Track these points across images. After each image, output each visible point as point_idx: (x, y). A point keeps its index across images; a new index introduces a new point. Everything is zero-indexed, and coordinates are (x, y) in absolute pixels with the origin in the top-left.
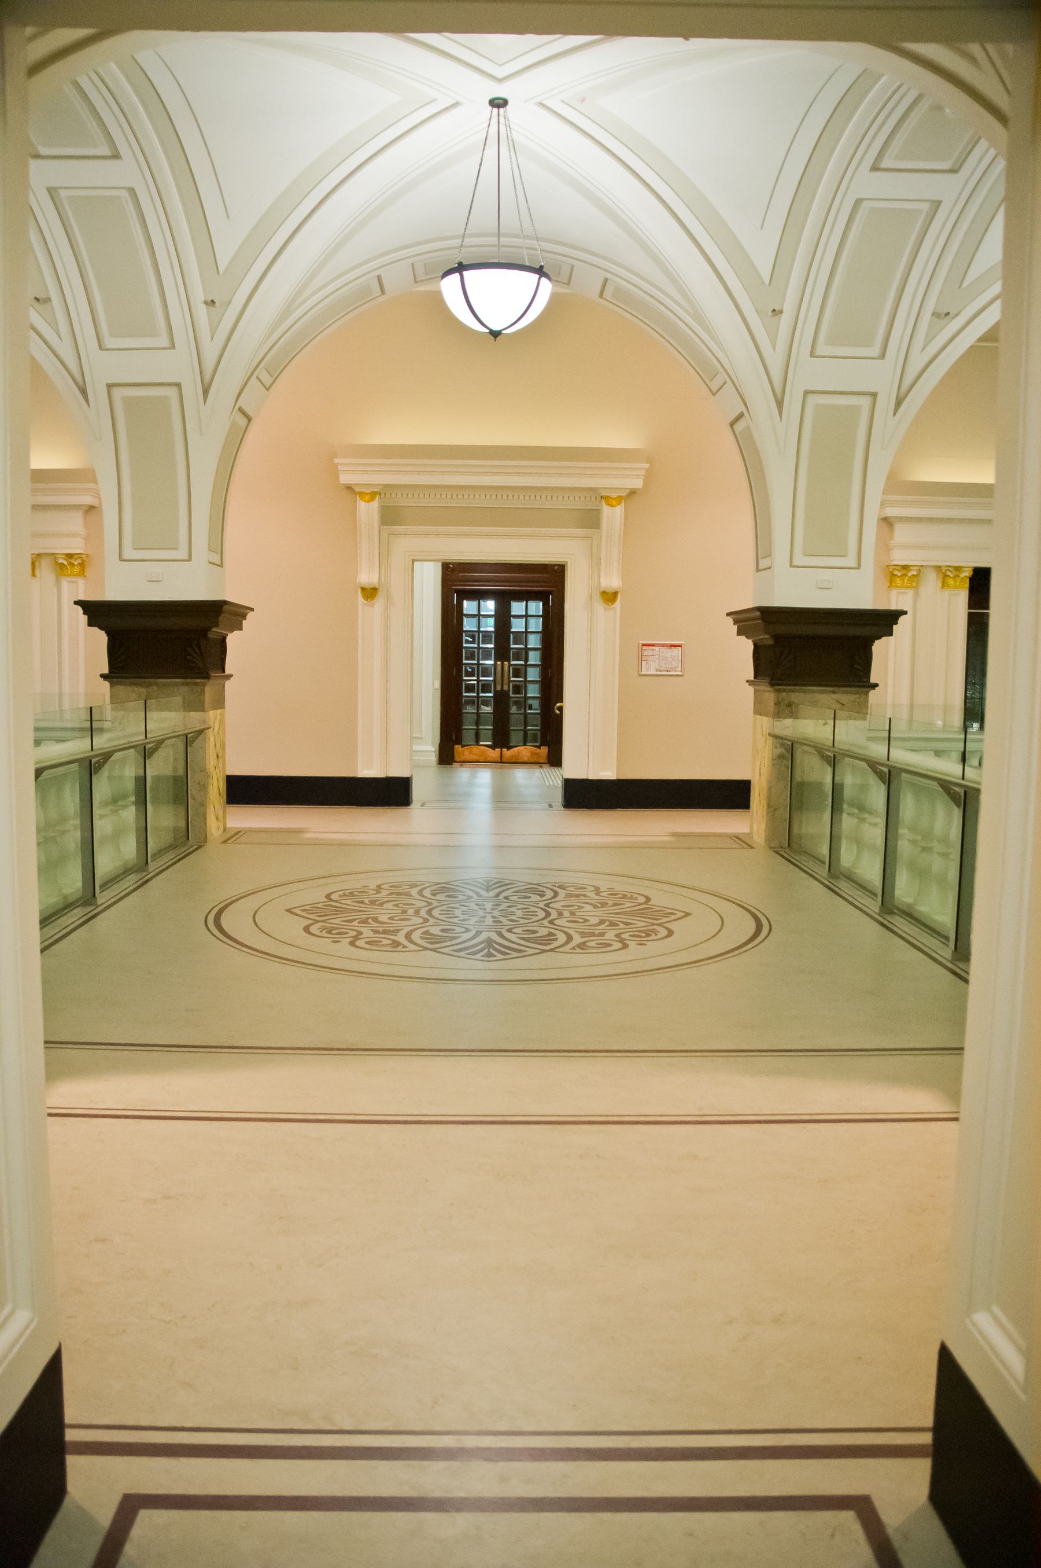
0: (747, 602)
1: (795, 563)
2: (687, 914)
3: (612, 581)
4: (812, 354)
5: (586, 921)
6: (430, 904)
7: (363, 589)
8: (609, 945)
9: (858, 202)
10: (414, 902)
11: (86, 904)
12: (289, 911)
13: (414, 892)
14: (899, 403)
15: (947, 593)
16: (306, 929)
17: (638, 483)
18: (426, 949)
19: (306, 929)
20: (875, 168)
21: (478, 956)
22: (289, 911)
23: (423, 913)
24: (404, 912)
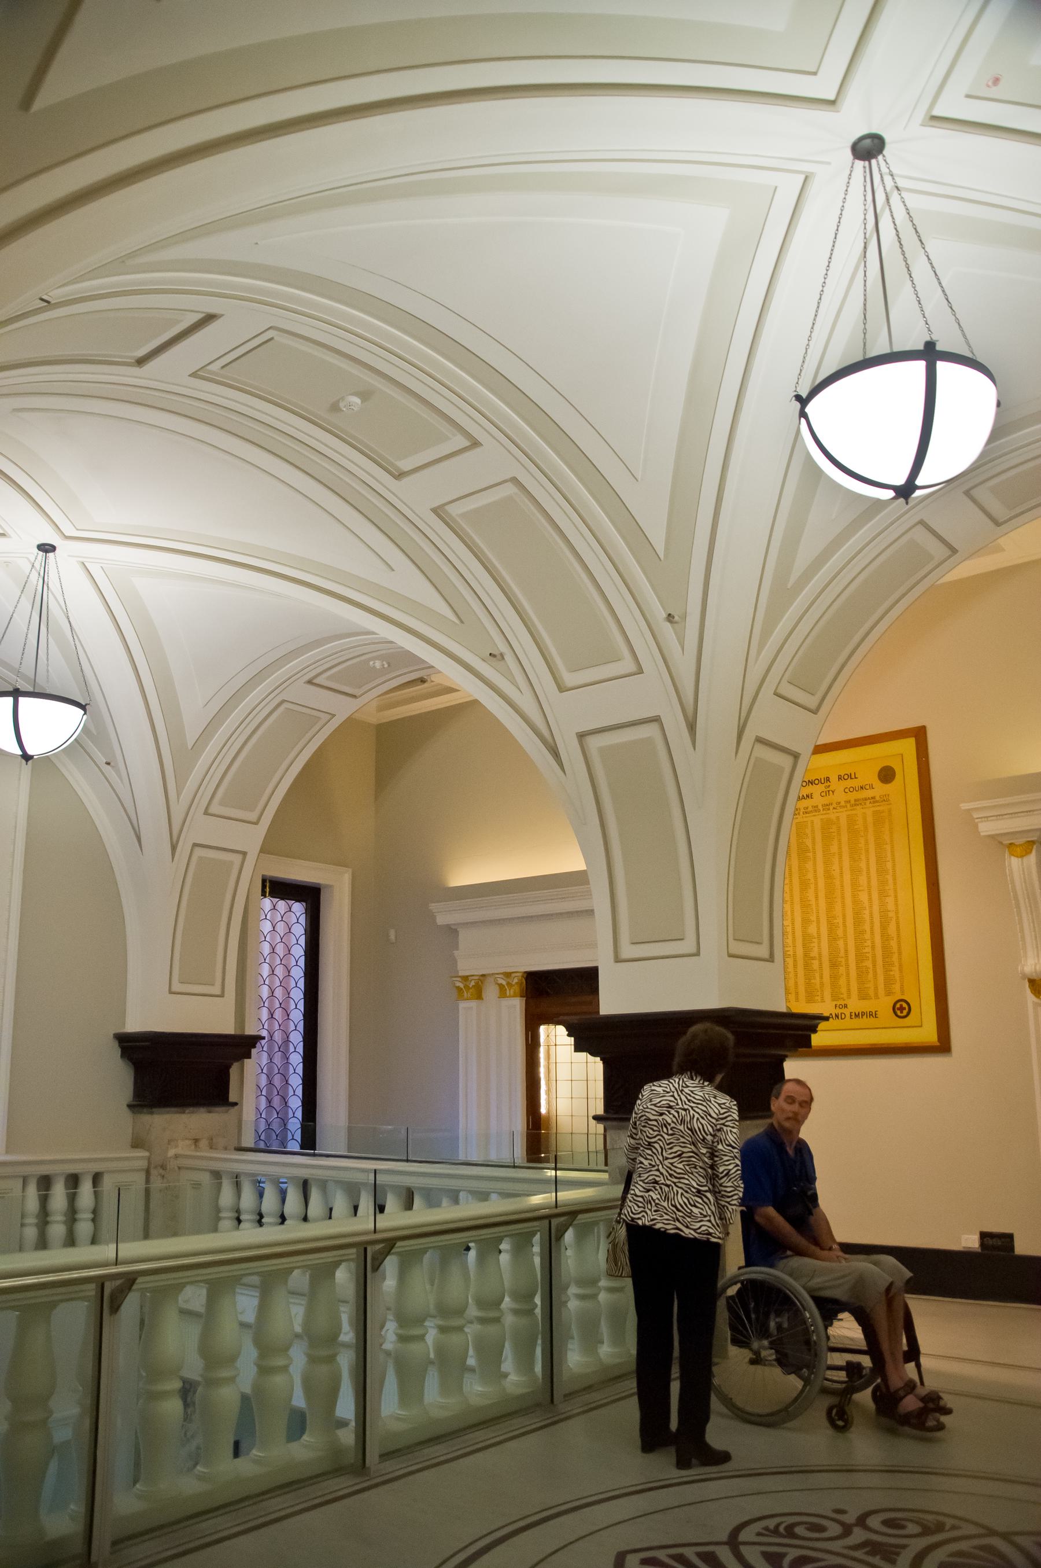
7: (1032, 982)
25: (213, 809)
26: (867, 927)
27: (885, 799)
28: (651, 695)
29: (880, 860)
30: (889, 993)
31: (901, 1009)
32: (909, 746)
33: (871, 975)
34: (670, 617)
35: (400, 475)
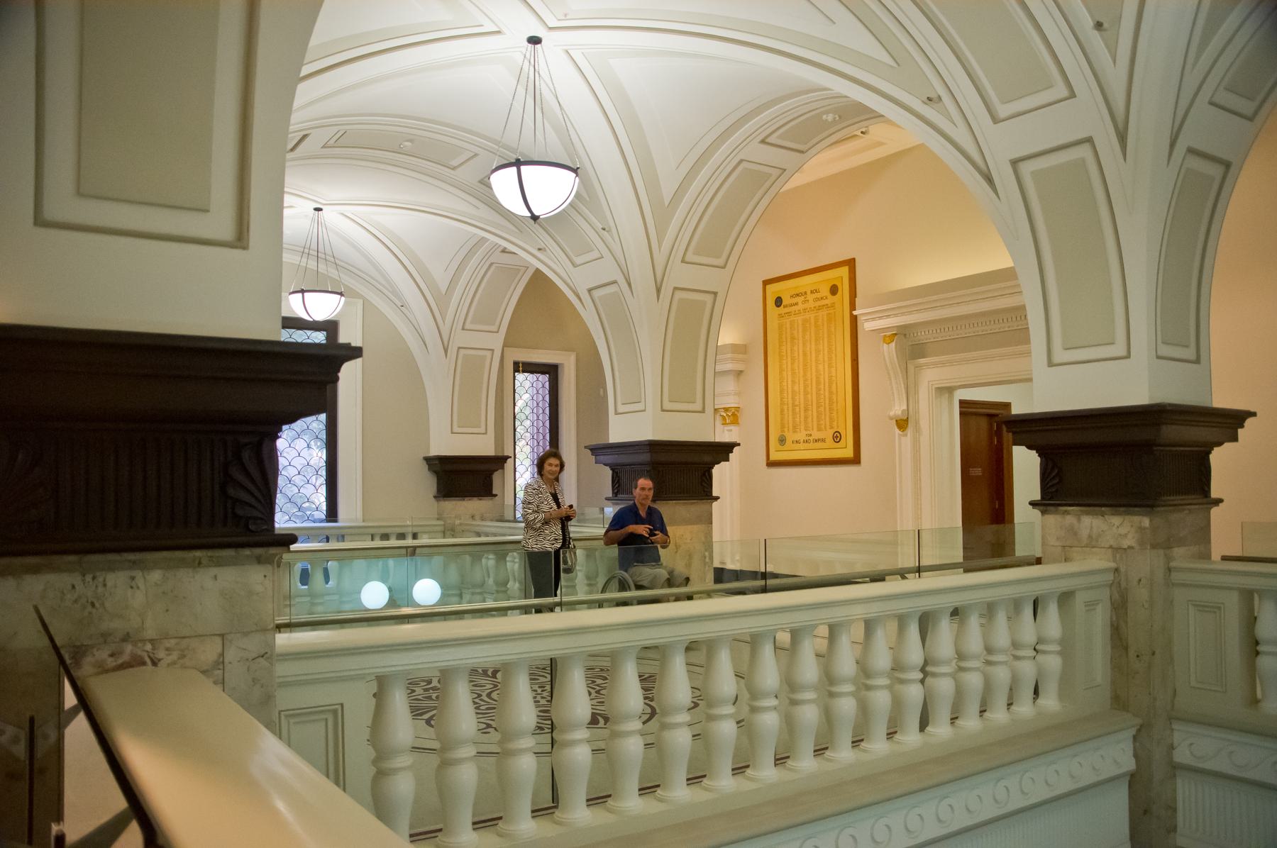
25: (467, 326)
27: (833, 305)
29: (829, 342)
30: (832, 428)
31: (837, 437)
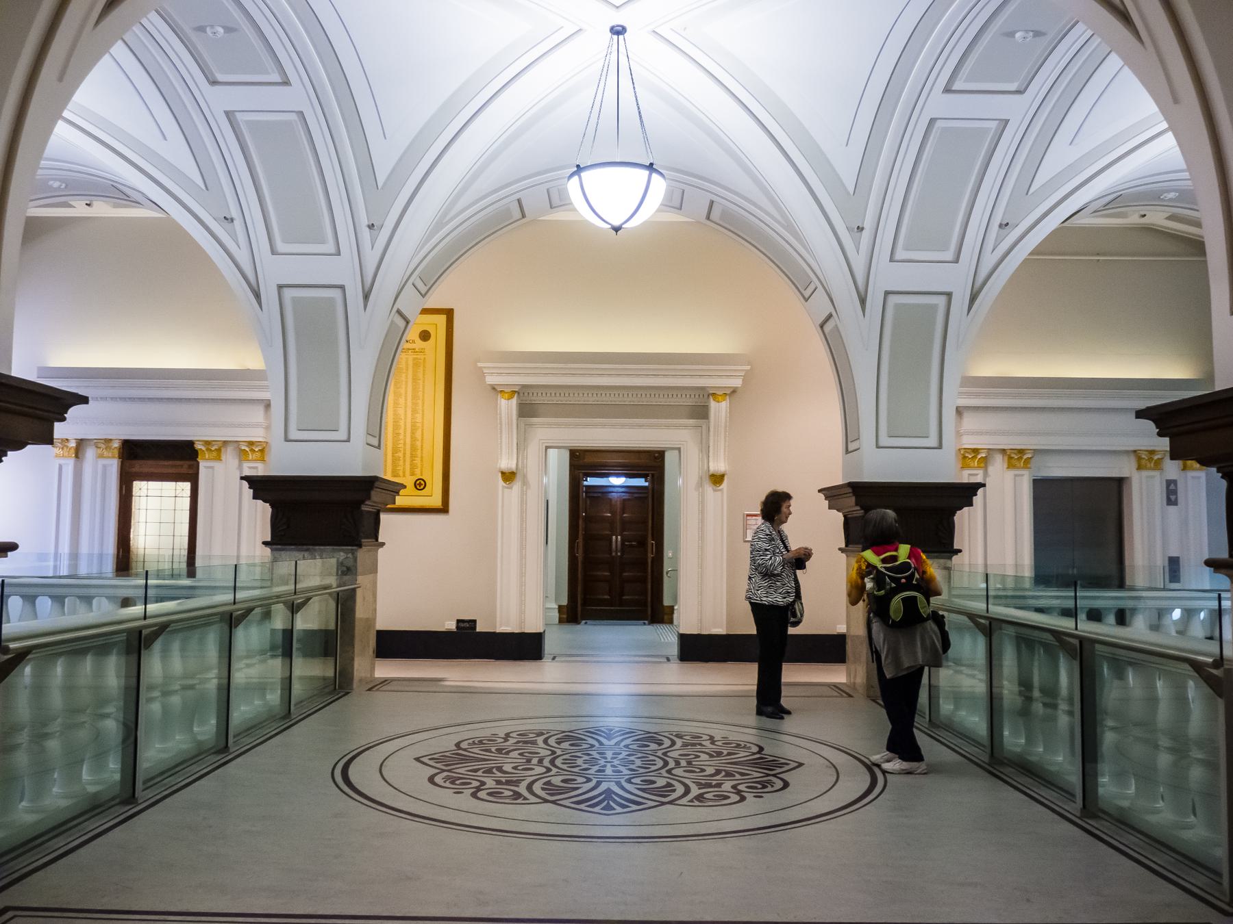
0: (839, 480)
1: (881, 444)
2: (801, 765)
3: (718, 466)
4: (891, 260)
5: (703, 770)
6: (554, 753)
7: (503, 473)
8: (727, 797)
9: (932, 121)
10: (539, 750)
11: (219, 752)
12: (418, 759)
13: (540, 740)
14: (973, 299)
15: (1012, 473)
16: (431, 780)
17: (737, 382)
18: (546, 801)
19: (431, 780)
20: (947, 90)
21: (597, 809)
22: (418, 759)
23: (546, 763)
24: (529, 761)
26: (401, 431)
27: (422, 351)
28: (343, 271)
29: (415, 389)
30: (412, 474)
31: (420, 485)
32: (443, 318)
33: (401, 462)
34: (371, 226)
35: (214, 83)
